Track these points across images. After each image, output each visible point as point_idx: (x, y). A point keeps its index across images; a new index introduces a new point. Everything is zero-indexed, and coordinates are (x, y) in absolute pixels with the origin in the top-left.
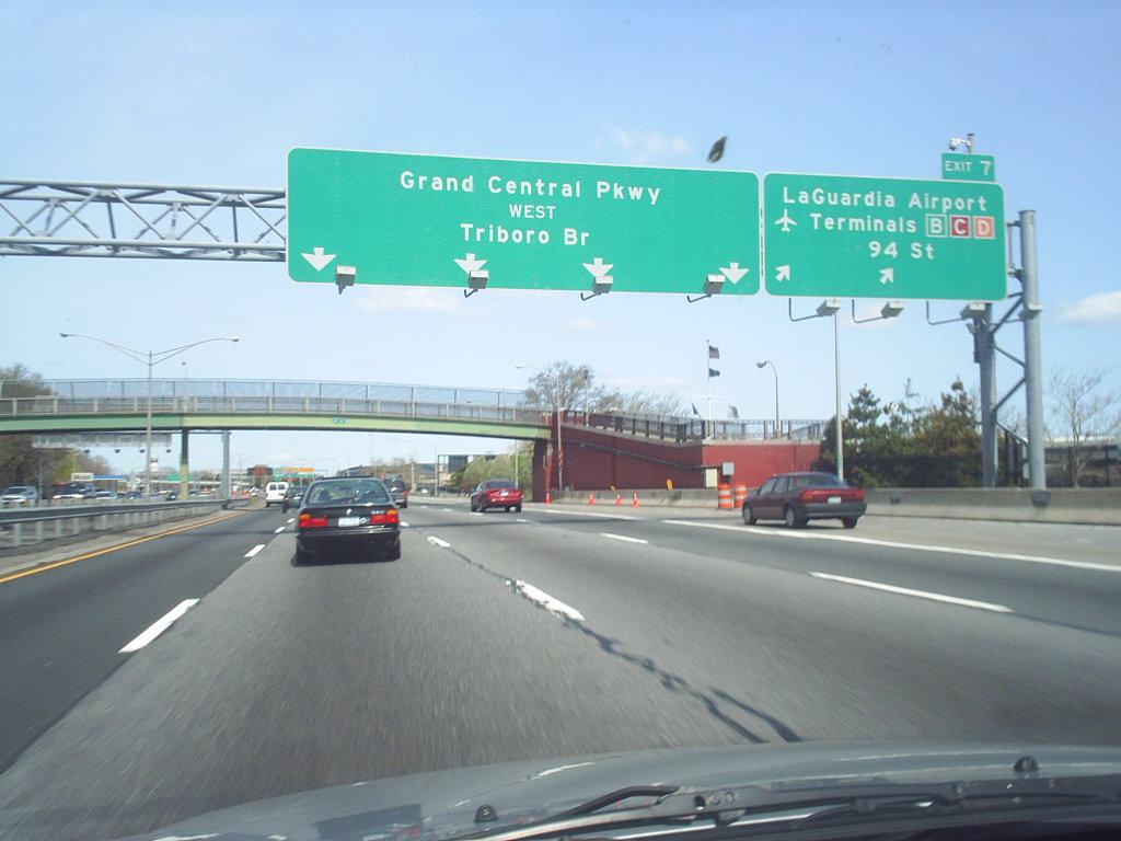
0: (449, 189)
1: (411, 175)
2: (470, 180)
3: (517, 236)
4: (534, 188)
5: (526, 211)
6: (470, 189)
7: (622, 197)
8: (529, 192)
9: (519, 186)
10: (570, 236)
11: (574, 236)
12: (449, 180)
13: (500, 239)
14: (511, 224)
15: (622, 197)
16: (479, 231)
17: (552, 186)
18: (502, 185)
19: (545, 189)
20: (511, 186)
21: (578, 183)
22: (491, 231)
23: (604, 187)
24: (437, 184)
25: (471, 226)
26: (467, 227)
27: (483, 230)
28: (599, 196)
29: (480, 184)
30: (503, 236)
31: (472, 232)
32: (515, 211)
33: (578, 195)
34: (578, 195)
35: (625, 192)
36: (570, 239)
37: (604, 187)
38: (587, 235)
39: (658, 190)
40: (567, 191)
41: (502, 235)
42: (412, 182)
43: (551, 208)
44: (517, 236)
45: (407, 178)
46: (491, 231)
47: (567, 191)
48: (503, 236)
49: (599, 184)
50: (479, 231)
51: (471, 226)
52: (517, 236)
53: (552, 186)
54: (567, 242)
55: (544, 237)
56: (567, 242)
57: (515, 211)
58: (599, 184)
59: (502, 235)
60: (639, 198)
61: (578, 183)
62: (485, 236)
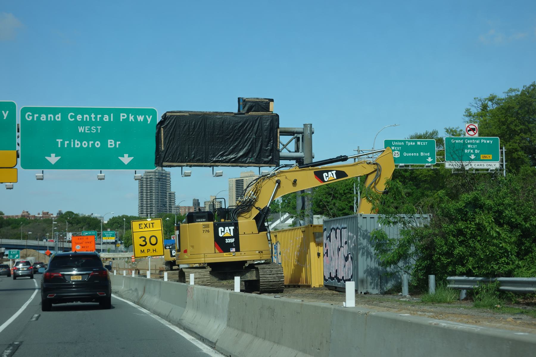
0: (49, 120)
1: (31, 114)
2: (59, 115)
3: (85, 144)
4: (91, 118)
5: (86, 129)
6: (60, 120)
7: (133, 120)
8: (88, 120)
9: (83, 117)
10: (111, 143)
11: (113, 143)
12: (49, 116)
13: (76, 146)
14: (83, 137)
15: (133, 120)
16: (66, 142)
17: (99, 116)
18: (75, 117)
19: (96, 118)
20: (79, 117)
21: (112, 114)
22: (72, 142)
23: (123, 116)
24: (43, 118)
25: (62, 140)
26: (59, 141)
27: (68, 142)
28: (121, 120)
29: (64, 117)
30: (78, 144)
31: (63, 144)
32: (81, 129)
33: (112, 120)
34: (112, 120)
35: (135, 118)
36: (111, 145)
37: (123, 116)
38: (120, 142)
39: (151, 116)
40: (106, 118)
41: (77, 144)
42: (31, 118)
43: (99, 127)
44: (85, 144)
45: (29, 115)
46: (72, 142)
47: (106, 118)
48: (78, 144)
49: (122, 114)
50: (66, 142)
51: (62, 140)
52: (85, 144)
53: (99, 116)
54: (109, 146)
55: (98, 144)
56: (109, 146)
57: (81, 129)
58: (122, 114)
59: (77, 144)
60: (142, 121)
61: (112, 114)
62: (69, 145)
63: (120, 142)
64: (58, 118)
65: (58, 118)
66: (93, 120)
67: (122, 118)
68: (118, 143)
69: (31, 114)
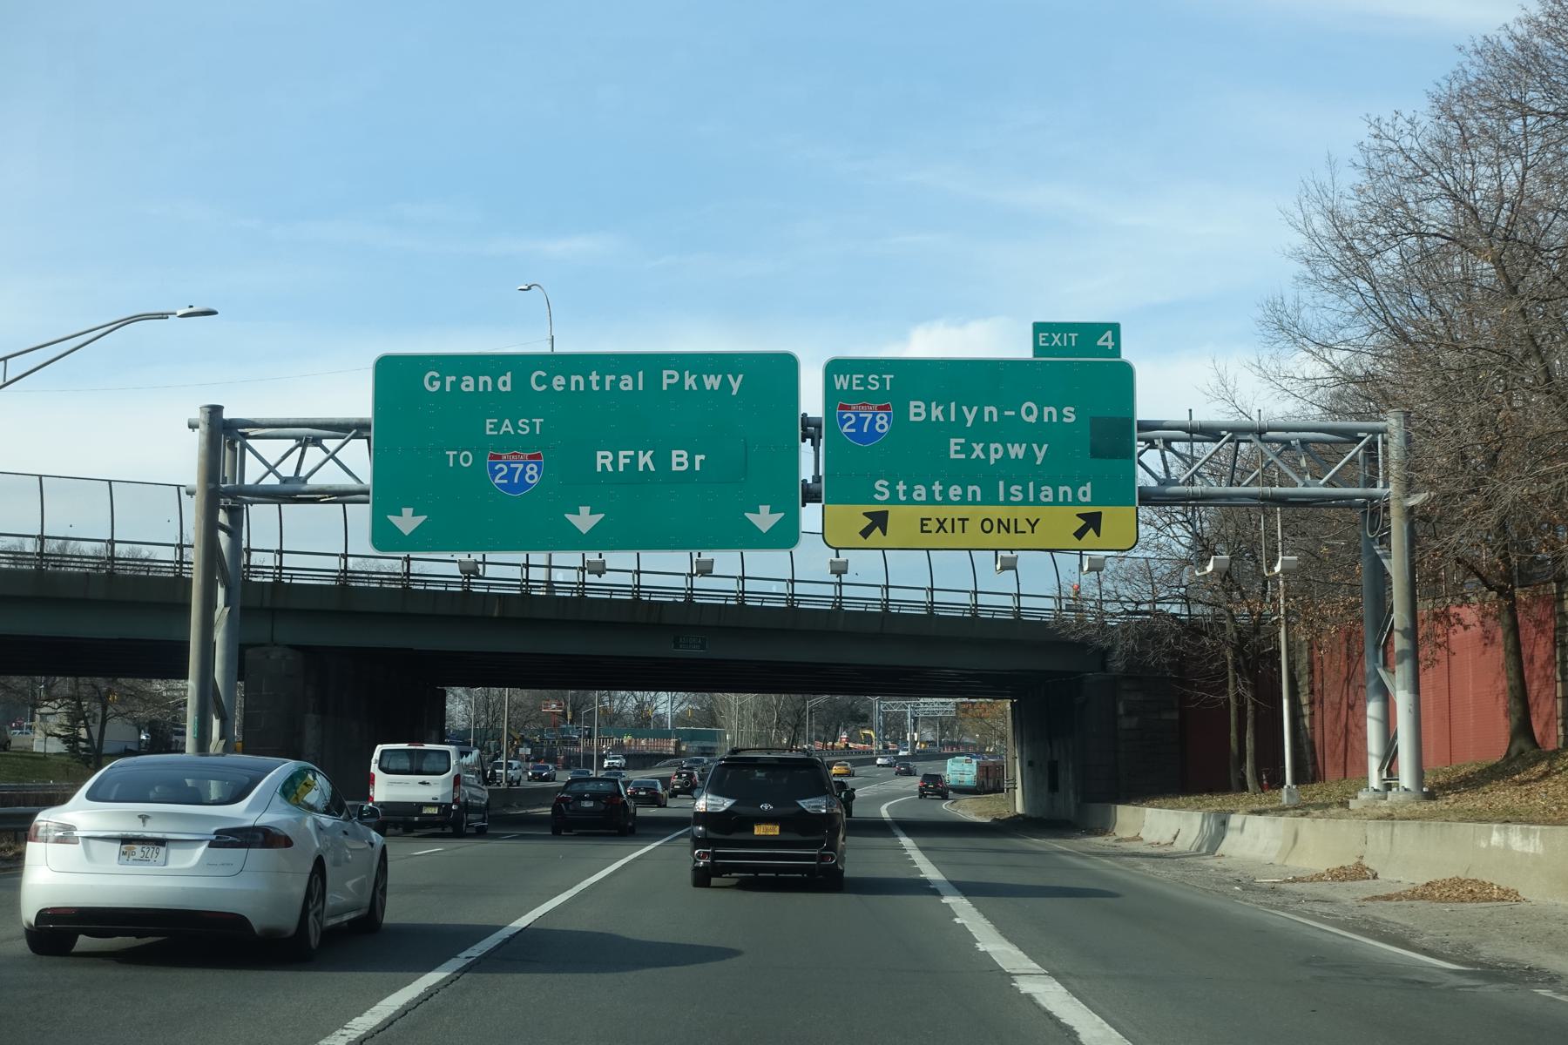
1: (437, 375)
2: (508, 377)
4: (588, 383)
6: (508, 388)
9: (568, 381)
17: (609, 378)
18: (547, 381)
19: (601, 383)
21: (641, 373)
24: (468, 384)
37: (672, 377)
38: (703, 457)
42: (437, 384)
45: (432, 379)
49: (665, 373)
53: (609, 378)
58: (665, 373)
61: (641, 373)
63: (703, 457)
64: (504, 384)
65: (504, 384)
66: (595, 388)
67: (666, 381)
68: (698, 458)
69: (437, 375)
